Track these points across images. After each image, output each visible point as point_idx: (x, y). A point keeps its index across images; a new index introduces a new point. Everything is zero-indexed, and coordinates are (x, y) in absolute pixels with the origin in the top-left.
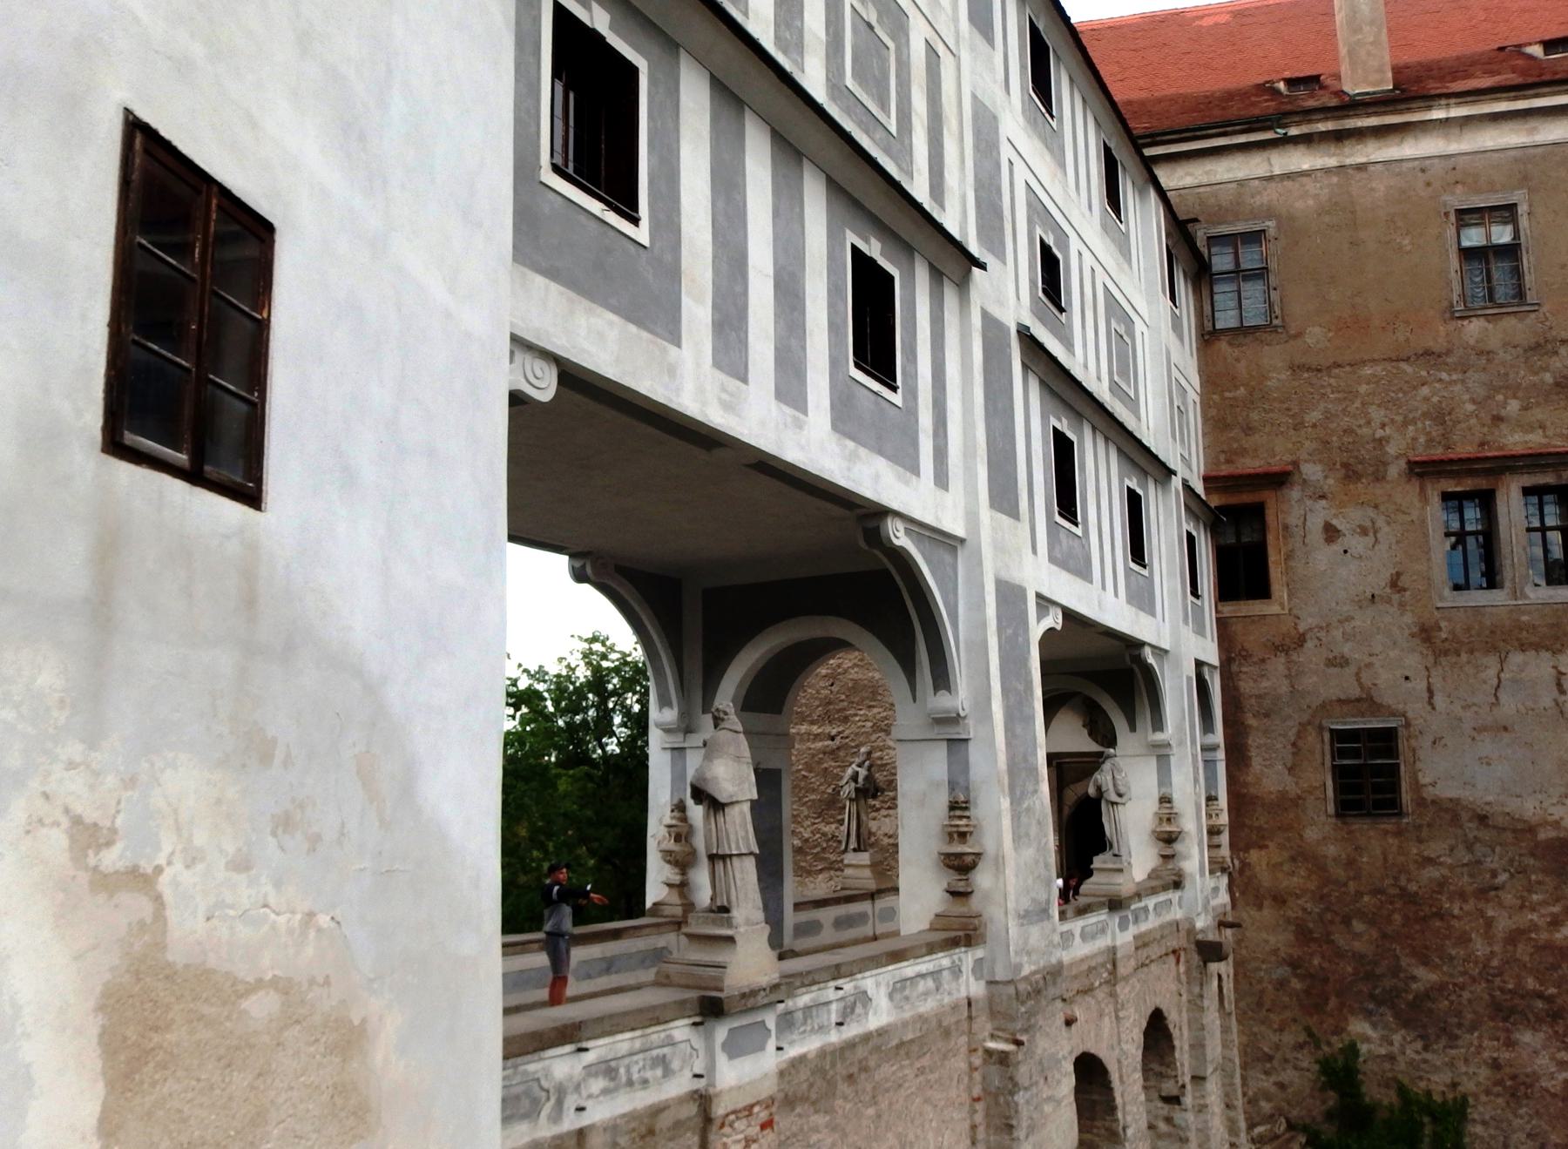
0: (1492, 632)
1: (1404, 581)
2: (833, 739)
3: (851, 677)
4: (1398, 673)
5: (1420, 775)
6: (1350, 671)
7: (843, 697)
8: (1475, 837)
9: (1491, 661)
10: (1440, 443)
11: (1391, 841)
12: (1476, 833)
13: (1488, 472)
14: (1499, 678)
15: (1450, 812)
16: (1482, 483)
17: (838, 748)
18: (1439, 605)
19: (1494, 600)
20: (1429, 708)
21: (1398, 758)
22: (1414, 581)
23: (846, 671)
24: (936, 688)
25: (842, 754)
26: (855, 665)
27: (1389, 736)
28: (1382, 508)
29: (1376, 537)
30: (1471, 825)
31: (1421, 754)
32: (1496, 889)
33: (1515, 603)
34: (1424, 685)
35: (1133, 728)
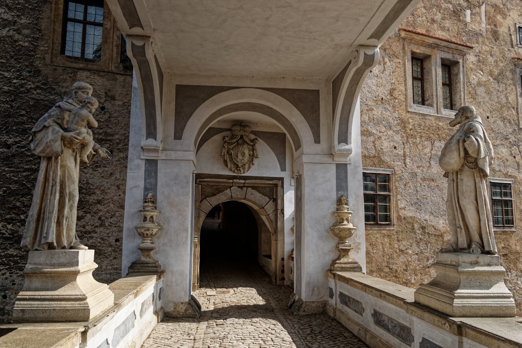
0: (429, 129)
1: (396, 94)
2: (9, 147)
3: (33, 96)
4: (392, 144)
5: (399, 202)
6: (371, 139)
7: (23, 112)
8: (420, 239)
10: (411, 24)
12: (420, 236)
13: (430, 46)
14: (431, 153)
15: (410, 222)
16: (427, 51)
17: (14, 156)
18: (409, 110)
19: (430, 112)
20: (404, 165)
22: (400, 95)
23: (28, 91)
25: (16, 161)
26: (38, 87)
27: (386, 178)
28: (387, 51)
29: (384, 67)
30: (418, 232)
32: (428, 267)
33: (437, 115)
34: (401, 153)
35: (317, 140)
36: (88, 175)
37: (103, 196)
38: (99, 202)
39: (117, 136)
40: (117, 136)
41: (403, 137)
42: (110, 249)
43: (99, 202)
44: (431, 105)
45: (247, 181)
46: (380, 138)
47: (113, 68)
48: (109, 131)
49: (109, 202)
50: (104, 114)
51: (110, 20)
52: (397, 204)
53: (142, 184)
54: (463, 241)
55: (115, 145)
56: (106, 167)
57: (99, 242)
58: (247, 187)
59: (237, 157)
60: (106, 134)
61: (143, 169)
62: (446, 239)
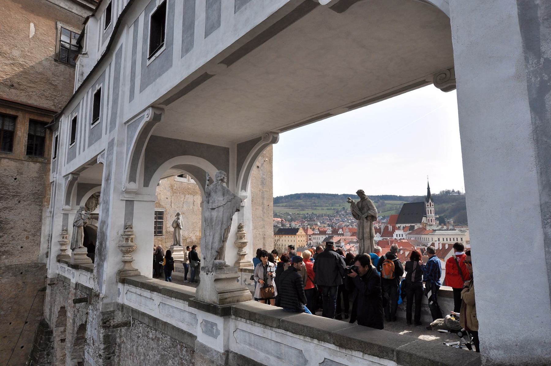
5: (167, 224)
9: (183, 196)
11: (160, 242)
21: (163, 219)
24: (242, 189)
31: (168, 218)
34: (170, 200)
36: (6, 214)
37: (14, 225)
38: (12, 228)
39: (23, 194)
40: (23, 194)
41: (171, 193)
42: (18, 252)
43: (12, 228)
44: (186, 178)
45: (93, 216)
46: (160, 194)
47: (22, 157)
48: (19, 191)
49: (18, 228)
50: (16, 182)
51: (21, 132)
52: (166, 225)
53: (61, 224)
54: (176, 244)
55: (22, 198)
56: (16, 210)
57: (12, 249)
58: (93, 219)
59: (89, 204)
60: (17, 192)
61: (62, 217)
62: (188, 241)
